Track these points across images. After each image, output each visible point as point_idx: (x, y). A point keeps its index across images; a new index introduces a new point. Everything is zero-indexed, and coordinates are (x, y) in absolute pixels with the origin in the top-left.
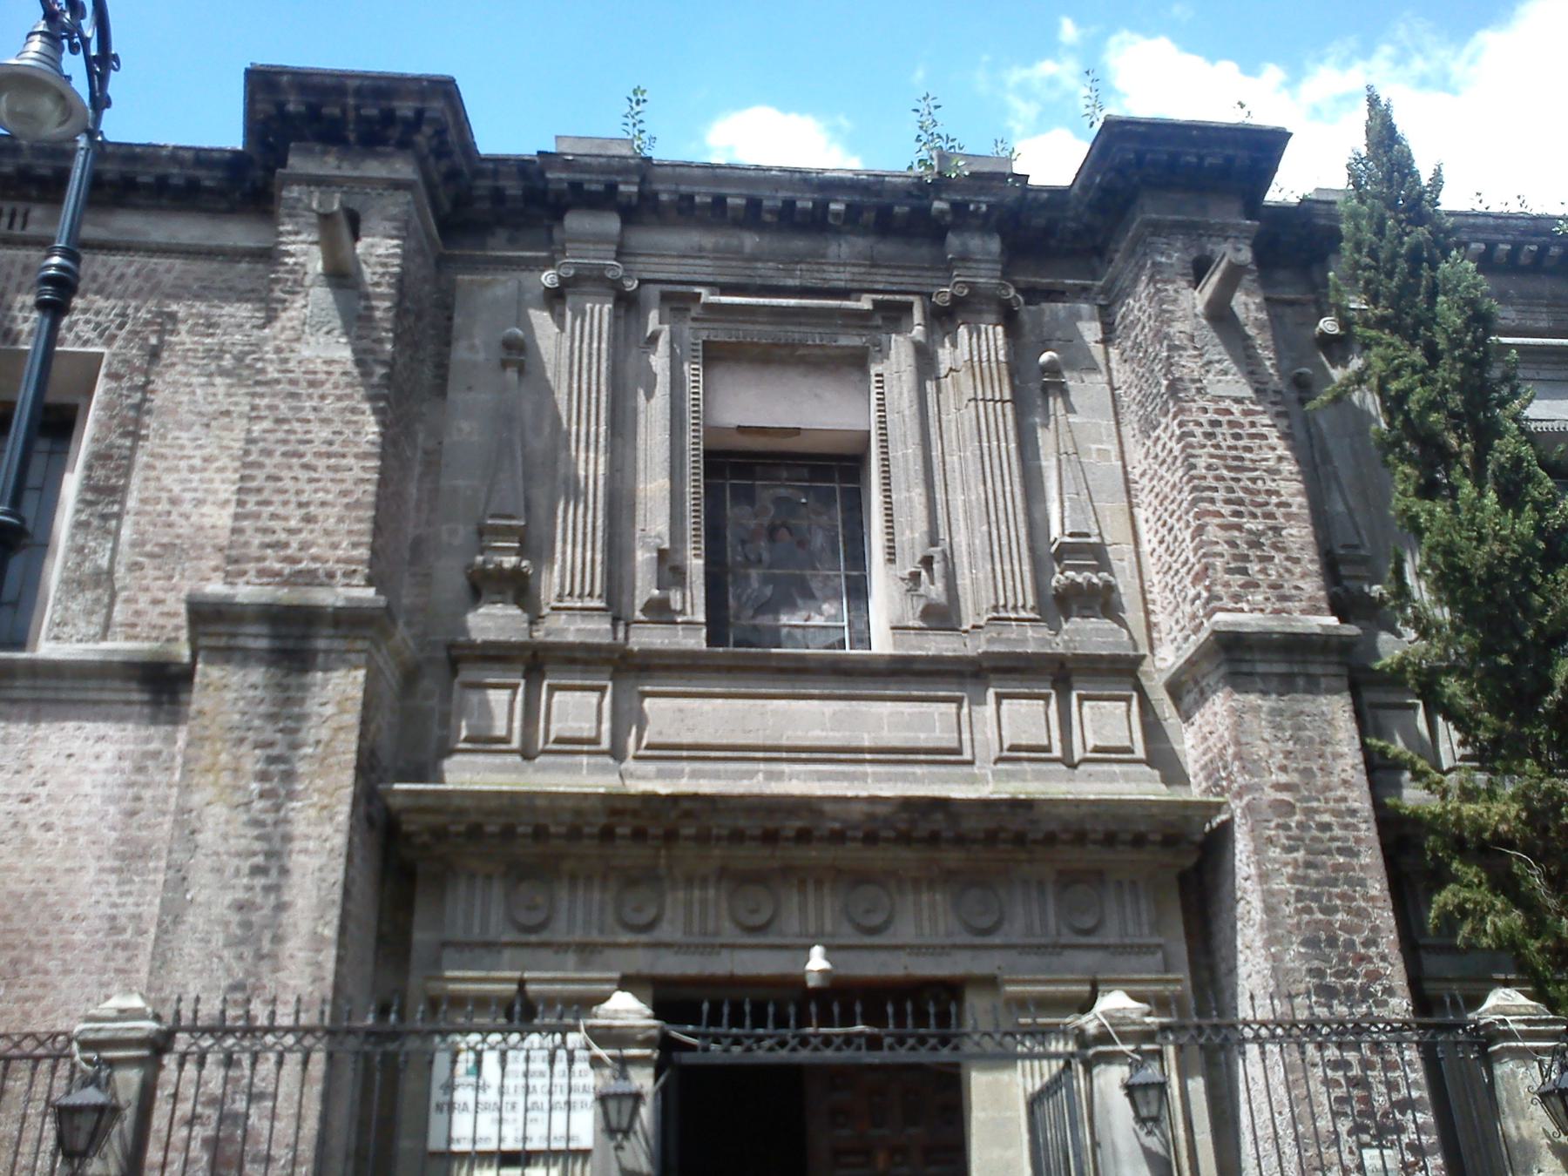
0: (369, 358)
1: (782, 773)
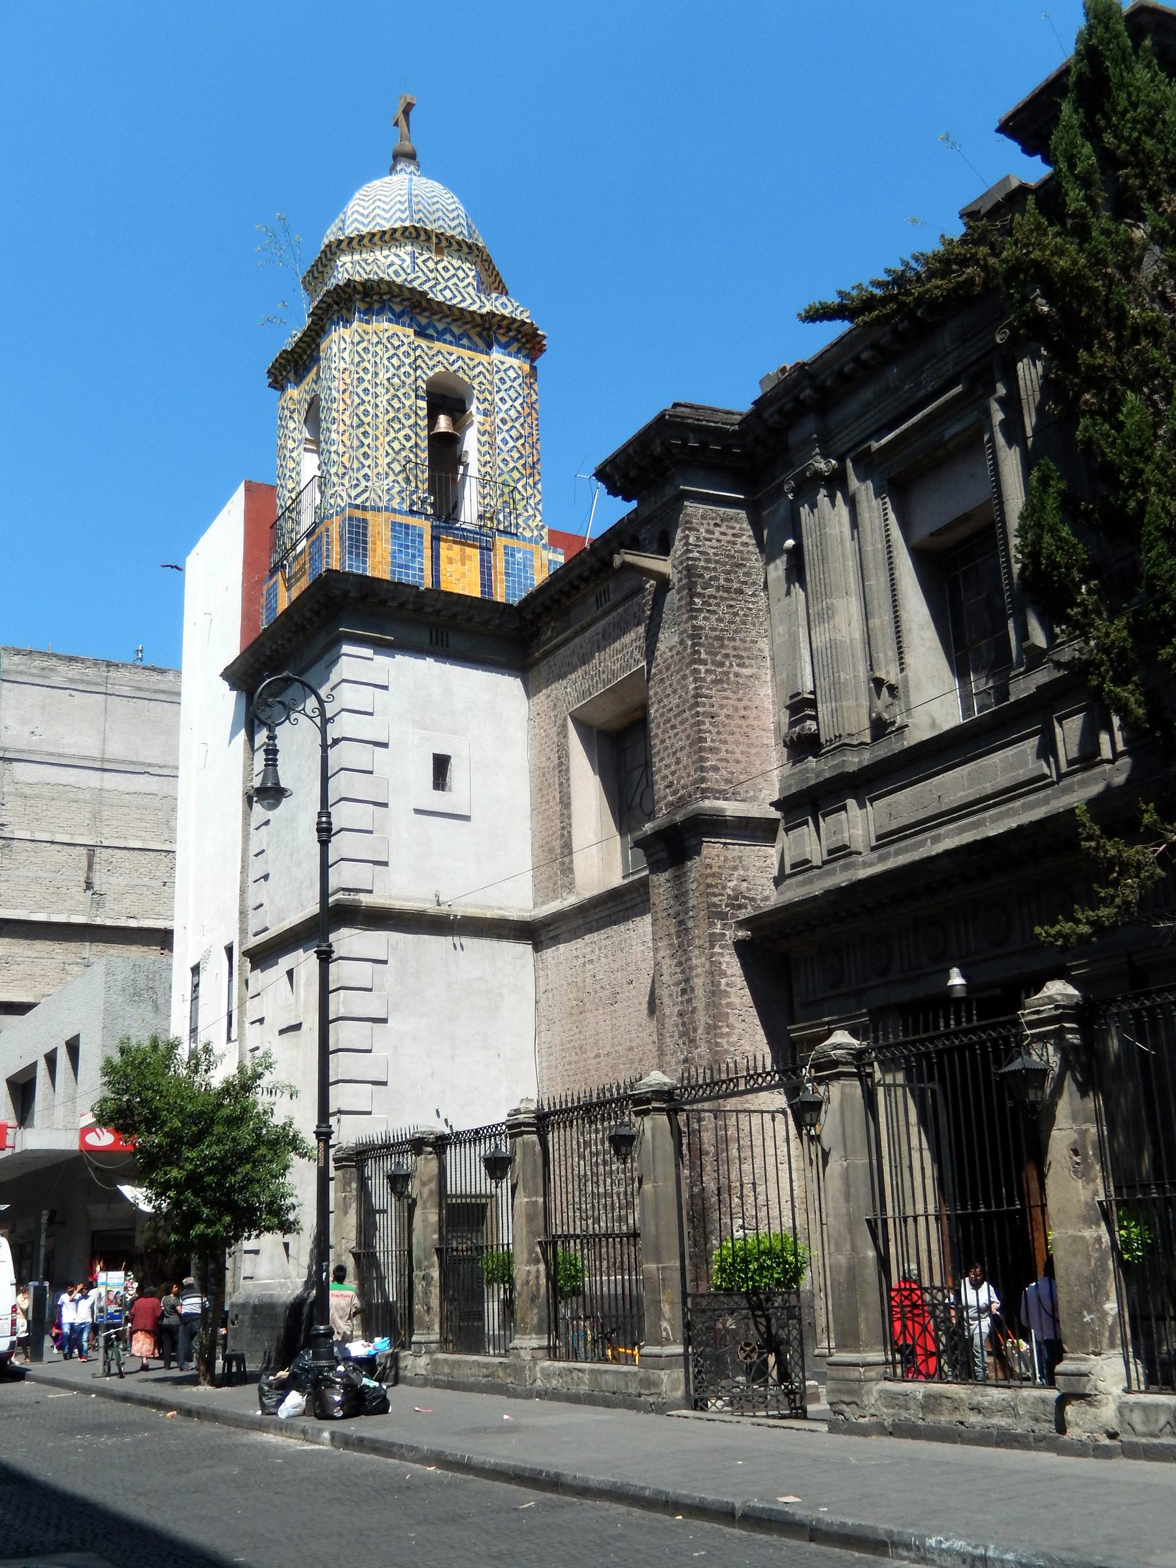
1: (939, 835)
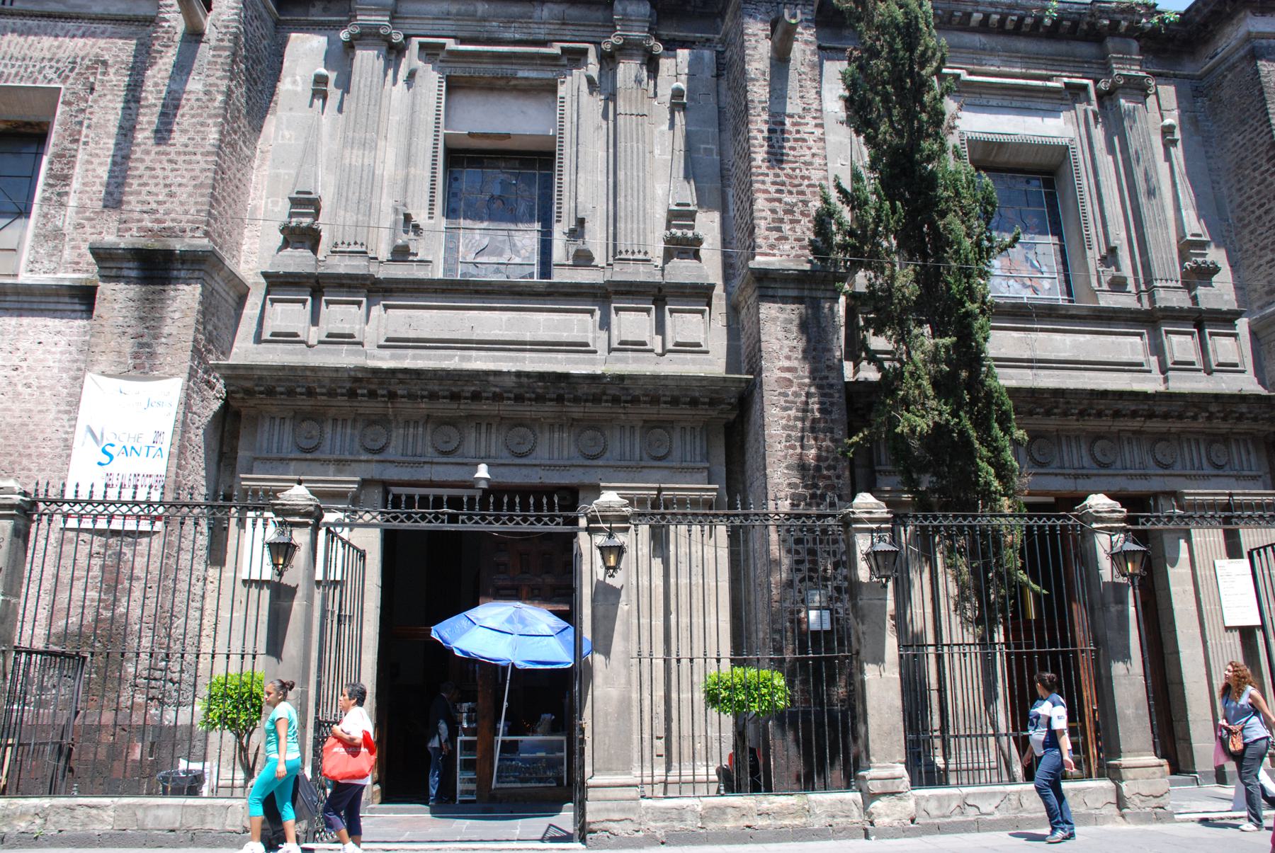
0: (213, 89)
1: (471, 356)
